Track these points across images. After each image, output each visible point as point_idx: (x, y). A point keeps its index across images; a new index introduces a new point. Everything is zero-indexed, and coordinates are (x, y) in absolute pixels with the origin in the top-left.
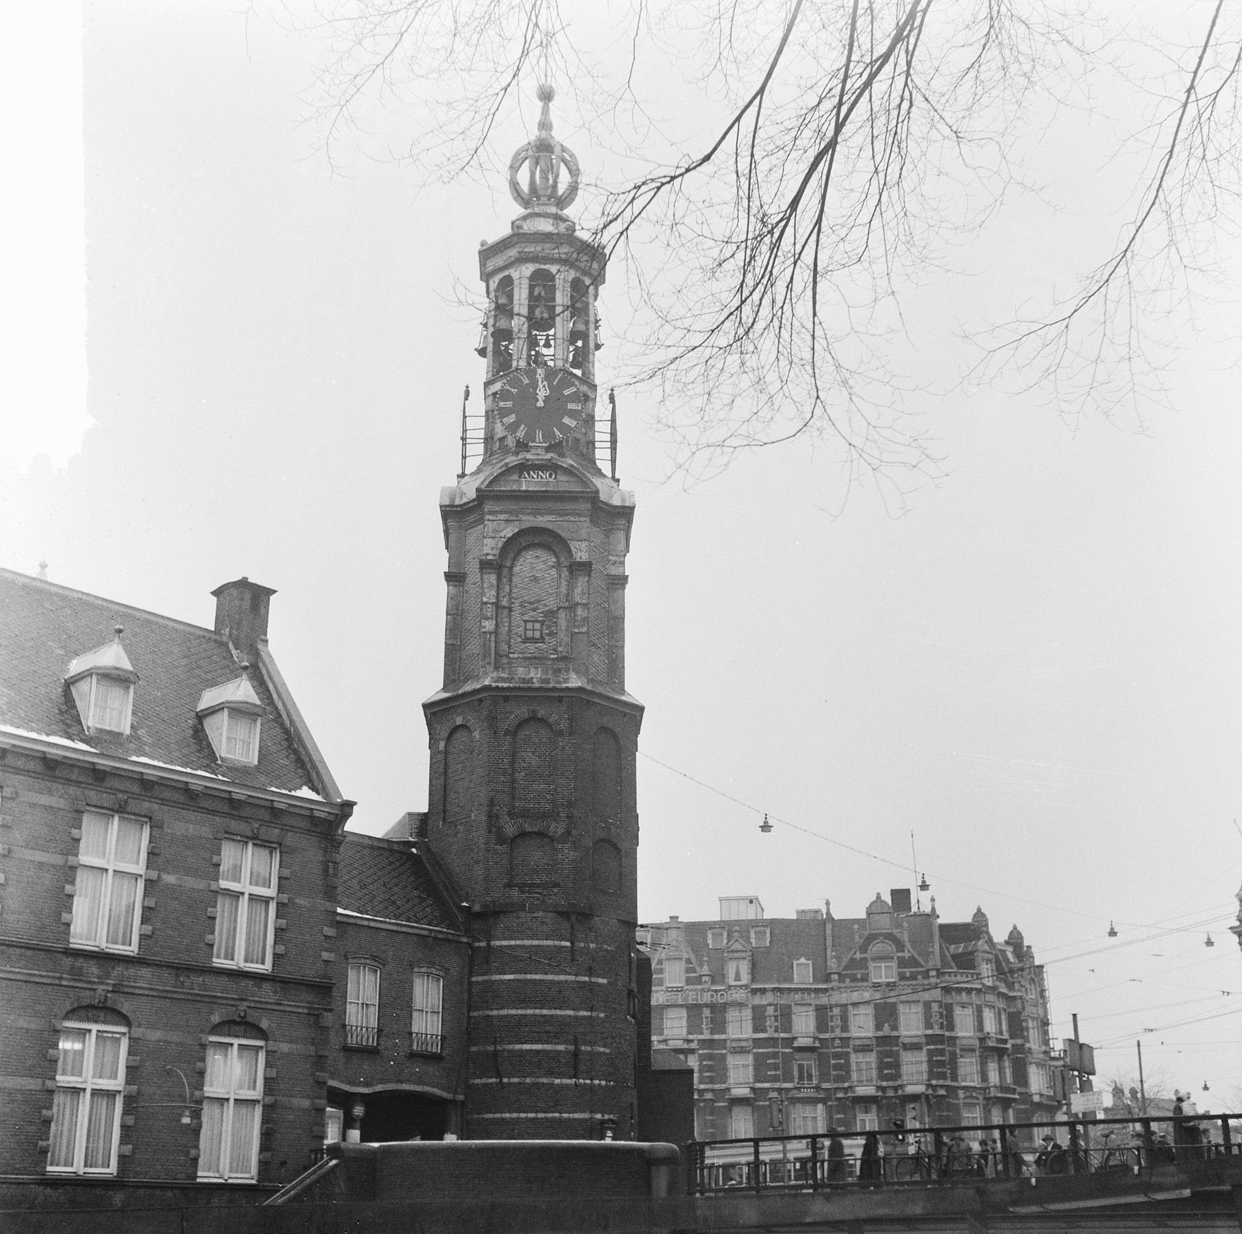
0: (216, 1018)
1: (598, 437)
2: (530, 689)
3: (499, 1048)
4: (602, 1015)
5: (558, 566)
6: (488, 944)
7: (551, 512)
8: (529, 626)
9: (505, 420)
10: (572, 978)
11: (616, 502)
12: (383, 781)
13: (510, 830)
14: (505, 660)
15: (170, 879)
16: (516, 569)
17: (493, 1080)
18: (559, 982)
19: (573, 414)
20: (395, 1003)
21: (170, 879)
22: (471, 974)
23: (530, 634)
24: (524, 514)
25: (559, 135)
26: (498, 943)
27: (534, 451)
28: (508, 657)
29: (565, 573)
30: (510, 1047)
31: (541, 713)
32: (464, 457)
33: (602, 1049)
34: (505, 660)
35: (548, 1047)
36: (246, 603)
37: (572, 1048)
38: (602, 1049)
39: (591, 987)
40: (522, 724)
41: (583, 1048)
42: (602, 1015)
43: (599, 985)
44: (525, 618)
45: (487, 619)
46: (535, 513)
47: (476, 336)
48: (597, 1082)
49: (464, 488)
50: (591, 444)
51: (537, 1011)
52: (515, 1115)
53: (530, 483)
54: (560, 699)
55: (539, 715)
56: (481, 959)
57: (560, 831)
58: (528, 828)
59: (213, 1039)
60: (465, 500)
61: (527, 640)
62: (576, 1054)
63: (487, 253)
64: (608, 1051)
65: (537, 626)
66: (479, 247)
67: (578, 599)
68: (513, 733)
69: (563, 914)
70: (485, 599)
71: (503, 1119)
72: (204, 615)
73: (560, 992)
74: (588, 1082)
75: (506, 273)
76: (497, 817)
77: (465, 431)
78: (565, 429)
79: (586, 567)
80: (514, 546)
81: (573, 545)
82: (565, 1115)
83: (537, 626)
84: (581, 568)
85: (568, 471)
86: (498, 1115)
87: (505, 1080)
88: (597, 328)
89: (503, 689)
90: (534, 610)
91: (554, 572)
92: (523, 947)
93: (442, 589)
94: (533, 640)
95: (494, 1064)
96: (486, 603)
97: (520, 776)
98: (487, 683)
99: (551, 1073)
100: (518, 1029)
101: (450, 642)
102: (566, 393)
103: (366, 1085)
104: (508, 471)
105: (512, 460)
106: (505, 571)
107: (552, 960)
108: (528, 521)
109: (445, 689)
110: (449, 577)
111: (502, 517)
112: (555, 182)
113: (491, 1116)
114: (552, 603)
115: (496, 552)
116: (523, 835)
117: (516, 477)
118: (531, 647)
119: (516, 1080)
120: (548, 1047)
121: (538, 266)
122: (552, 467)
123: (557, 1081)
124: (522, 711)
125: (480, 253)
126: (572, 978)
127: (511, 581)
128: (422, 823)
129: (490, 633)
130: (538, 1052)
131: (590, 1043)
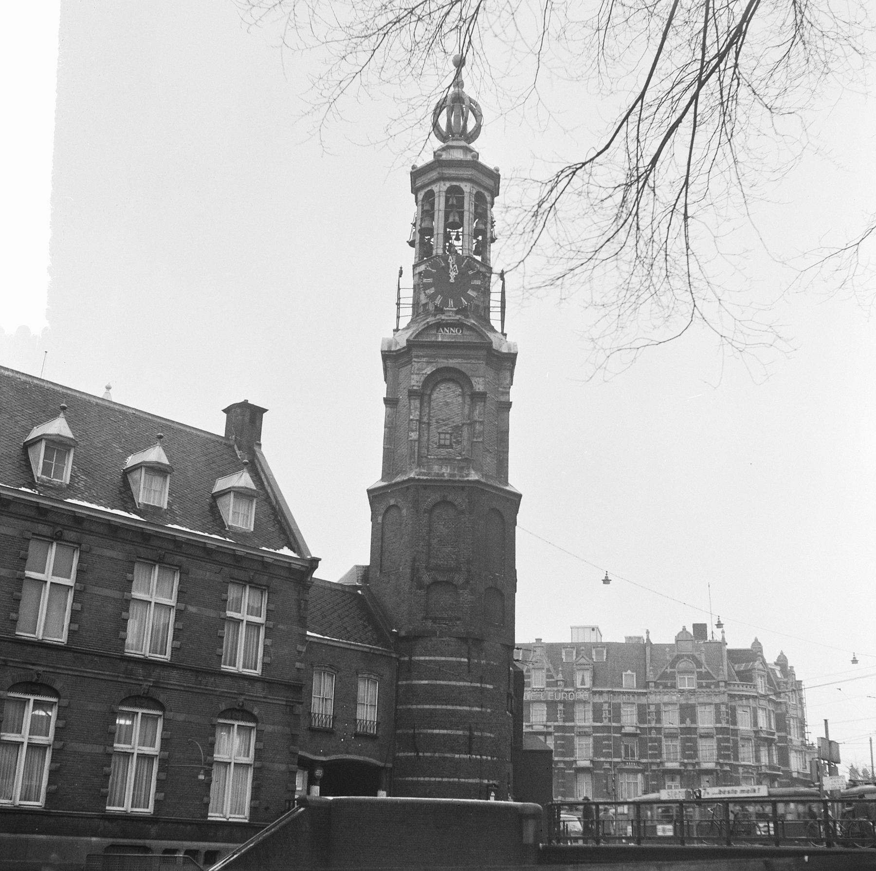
0: (223, 707)
1: (492, 304)
2: (442, 481)
3: (416, 731)
4: (489, 710)
5: (463, 395)
6: (410, 659)
8: (442, 436)
10: (468, 684)
11: (504, 350)
12: (339, 544)
13: (426, 579)
14: (424, 460)
15: (192, 609)
16: (434, 396)
17: (412, 754)
18: (460, 687)
19: (476, 288)
20: (346, 699)
21: (192, 609)
22: (398, 680)
23: (442, 442)
25: (468, 91)
26: (417, 658)
27: (447, 314)
28: (426, 457)
29: (468, 399)
30: (425, 731)
31: (450, 498)
32: (398, 317)
33: (489, 735)
34: (424, 460)
35: (449, 732)
36: (246, 419)
37: (467, 733)
38: (489, 735)
39: (482, 690)
40: (436, 505)
41: (475, 733)
42: (489, 710)
43: (488, 690)
44: (440, 430)
45: (413, 431)
47: (407, 232)
48: (484, 757)
50: (487, 309)
51: (444, 707)
52: (427, 779)
53: (444, 336)
54: (463, 488)
55: (448, 499)
56: (406, 669)
57: (461, 581)
58: (440, 579)
59: (221, 721)
61: (440, 446)
62: (471, 738)
64: (492, 736)
65: (448, 436)
66: (410, 169)
67: (476, 418)
68: (430, 511)
69: (464, 640)
70: (411, 417)
71: (418, 782)
72: (218, 426)
73: (460, 693)
74: (478, 757)
75: (429, 188)
76: (418, 570)
77: (399, 299)
78: (469, 298)
79: (482, 396)
81: (474, 380)
82: (463, 780)
83: (448, 436)
84: (478, 397)
85: (471, 328)
86: (415, 779)
87: (421, 754)
88: (492, 227)
89: (423, 480)
90: (445, 425)
91: (460, 399)
92: (435, 661)
93: (381, 410)
94: (444, 446)
95: (413, 743)
96: (412, 420)
97: (434, 541)
98: (412, 475)
99: (453, 750)
100: (432, 719)
101: (386, 447)
103: (325, 755)
104: (429, 327)
105: (431, 320)
106: (426, 398)
107: (454, 671)
108: (443, 363)
109: (383, 479)
110: (387, 401)
111: (424, 360)
113: (410, 779)
114: (458, 420)
116: (436, 583)
117: (434, 332)
118: (443, 451)
119: (429, 754)
120: (449, 732)
122: (459, 325)
123: (457, 756)
124: (436, 497)
125: (411, 173)
126: (468, 684)
127: (429, 403)
128: (365, 573)
129: (415, 441)
130: (444, 735)
131: (482, 730)
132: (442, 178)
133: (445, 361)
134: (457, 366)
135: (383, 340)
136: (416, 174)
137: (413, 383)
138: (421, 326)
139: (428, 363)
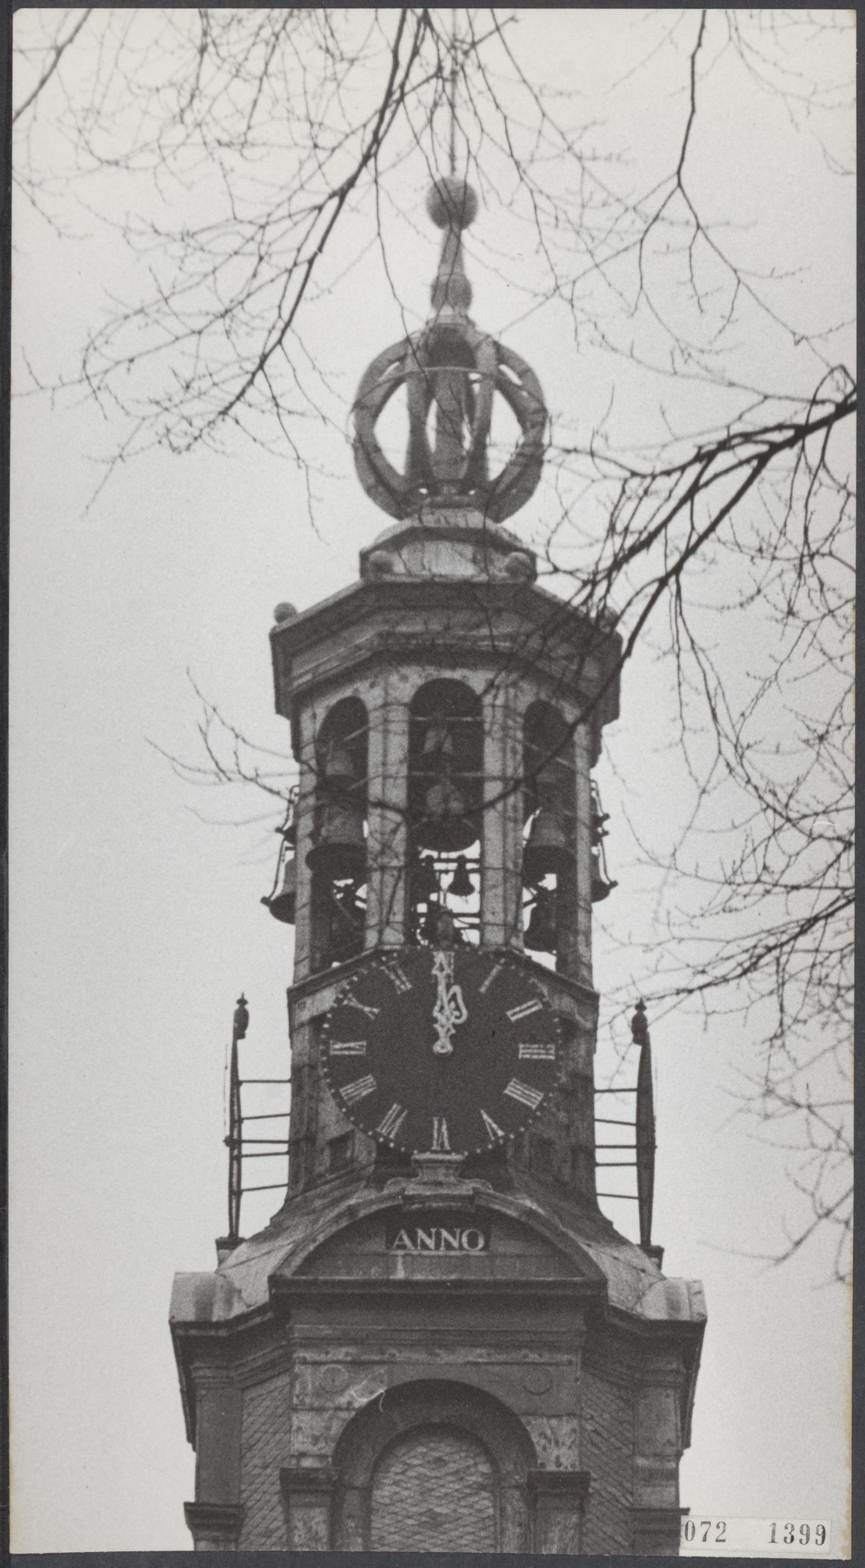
1: (602, 1134)
5: (495, 1485)
7: (472, 1339)
9: (347, 1091)
11: (654, 1309)
16: (383, 1494)
19: (534, 1074)
24: (400, 1345)
27: (426, 1176)
29: (515, 1504)
46: (433, 1341)
49: (236, 1276)
50: (584, 1155)
60: (238, 1309)
63: (294, 638)
66: (271, 623)
75: (348, 693)
80: (370, 1438)
81: (538, 1429)
85: (521, 1229)
88: (597, 838)
91: (485, 1503)
102: (515, 1015)
104: (357, 1228)
105: (363, 1198)
106: (352, 1500)
108: (416, 1364)
111: (341, 1353)
112: (480, 444)
115: (327, 1448)
117: (377, 1245)
121: (433, 673)
125: (275, 637)
132: (389, 656)
133: (422, 1356)
134: (473, 1378)
135: (179, 1284)
136: (294, 638)
137: (299, 1443)
138: (324, 1227)
139: (356, 1364)
